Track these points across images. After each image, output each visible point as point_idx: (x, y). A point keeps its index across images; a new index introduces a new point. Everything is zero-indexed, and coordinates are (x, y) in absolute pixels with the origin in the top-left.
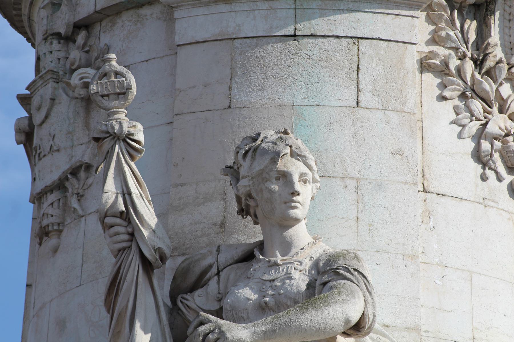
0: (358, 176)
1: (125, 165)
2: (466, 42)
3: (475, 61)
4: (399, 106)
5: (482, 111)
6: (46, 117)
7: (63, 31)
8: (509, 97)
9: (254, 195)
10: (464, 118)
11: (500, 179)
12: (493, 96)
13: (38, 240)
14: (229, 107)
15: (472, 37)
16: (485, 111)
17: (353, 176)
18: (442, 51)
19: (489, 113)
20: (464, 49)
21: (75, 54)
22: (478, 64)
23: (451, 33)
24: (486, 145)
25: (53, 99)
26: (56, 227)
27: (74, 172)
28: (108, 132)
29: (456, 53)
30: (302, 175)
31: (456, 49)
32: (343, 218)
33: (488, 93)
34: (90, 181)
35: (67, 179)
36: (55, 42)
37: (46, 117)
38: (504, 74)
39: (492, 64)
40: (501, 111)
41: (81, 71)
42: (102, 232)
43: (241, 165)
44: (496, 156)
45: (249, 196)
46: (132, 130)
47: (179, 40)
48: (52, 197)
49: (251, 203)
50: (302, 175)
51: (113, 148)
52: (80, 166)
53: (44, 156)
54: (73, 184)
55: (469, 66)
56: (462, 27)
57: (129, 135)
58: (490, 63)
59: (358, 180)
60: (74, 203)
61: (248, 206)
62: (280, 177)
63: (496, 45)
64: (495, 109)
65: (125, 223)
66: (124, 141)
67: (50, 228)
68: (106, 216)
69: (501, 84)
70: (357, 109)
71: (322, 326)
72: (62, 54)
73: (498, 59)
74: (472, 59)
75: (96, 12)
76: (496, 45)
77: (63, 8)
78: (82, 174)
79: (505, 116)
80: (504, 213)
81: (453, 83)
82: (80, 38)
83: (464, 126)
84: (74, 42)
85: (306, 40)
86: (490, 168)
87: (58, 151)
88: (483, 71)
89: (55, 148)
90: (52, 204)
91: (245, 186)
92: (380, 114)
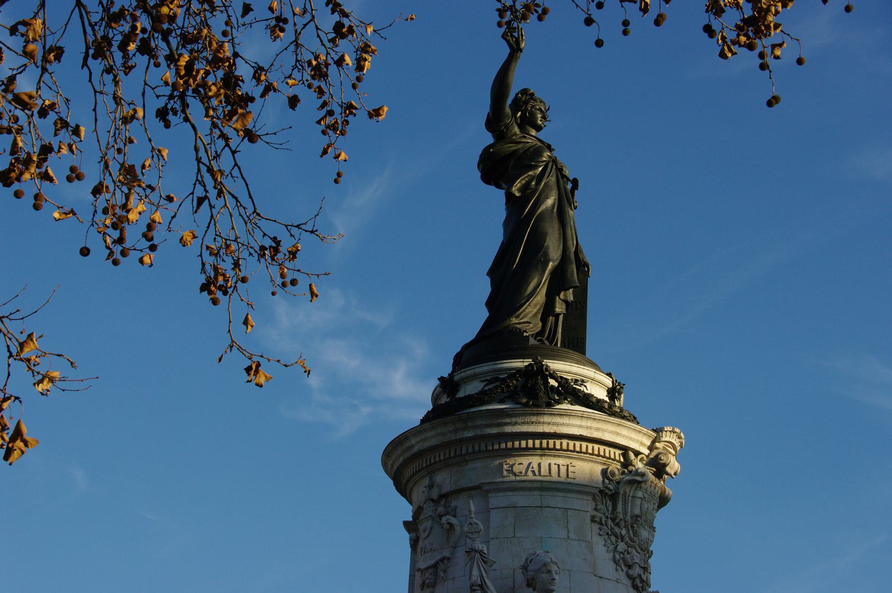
0: (569, 569)
1: (481, 565)
2: (608, 511)
3: (611, 519)
7: (435, 498)
8: (625, 535)
9: (535, 578)
10: (609, 544)
11: (622, 570)
12: (619, 535)
13: (421, 588)
14: (514, 537)
15: (610, 509)
16: (616, 541)
18: (599, 515)
19: (617, 541)
20: (607, 514)
21: (441, 509)
22: (613, 520)
23: (602, 507)
24: (617, 557)
25: (431, 528)
26: (432, 584)
27: (442, 560)
28: (472, 549)
29: (604, 515)
30: (556, 571)
31: (604, 514)
33: (617, 533)
35: (438, 563)
36: (431, 503)
37: (428, 536)
38: (623, 525)
39: (618, 521)
40: (622, 541)
41: (446, 517)
43: (529, 565)
44: (621, 561)
45: (533, 579)
46: (483, 549)
47: (490, 506)
48: (430, 571)
49: (533, 582)
50: (556, 571)
51: (475, 555)
52: (445, 558)
53: (427, 552)
54: (441, 566)
55: (610, 522)
56: (606, 504)
57: (482, 551)
58: (617, 521)
59: (569, 571)
60: (442, 574)
61: (532, 583)
63: (620, 513)
64: (620, 540)
65: (481, 589)
66: (479, 553)
67: (430, 584)
68: (473, 586)
69: (622, 529)
72: (434, 508)
73: (620, 519)
74: (611, 518)
75: (451, 491)
76: (620, 513)
77: (435, 488)
78: (446, 561)
79: (624, 543)
81: (603, 529)
82: (443, 502)
83: (608, 547)
84: (439, 503)
85: (546, 508)
86: (619, 566)
87: (434, 550)
88: (615, 523)
89: (433, 549)
90: (431, 574)
91: (531, 575)
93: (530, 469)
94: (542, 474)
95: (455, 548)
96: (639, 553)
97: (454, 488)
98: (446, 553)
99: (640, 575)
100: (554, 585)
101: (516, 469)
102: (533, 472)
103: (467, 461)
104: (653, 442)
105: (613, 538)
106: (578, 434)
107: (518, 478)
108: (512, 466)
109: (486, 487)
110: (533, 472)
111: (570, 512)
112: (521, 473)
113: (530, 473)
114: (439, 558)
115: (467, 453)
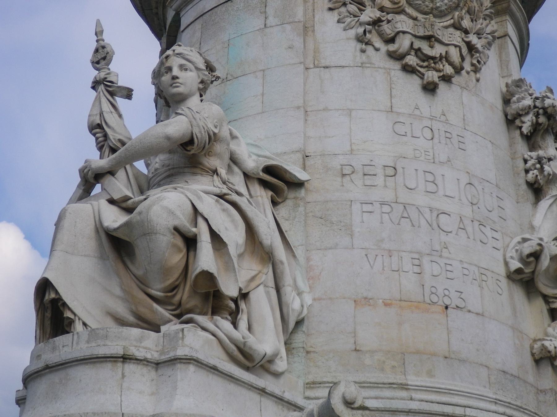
4: (291, 20)
5: (357, 10)
17: (261, 69)
32: (254, 96)
42: (217, 167)
59: (264, 71)
62: (168, 71)
70: (267, 30)
71: (148, 144)
80: (380, 70)
92: (279, 27)
96: (415, 19)
99: (418, 51)
100: (177, 87)
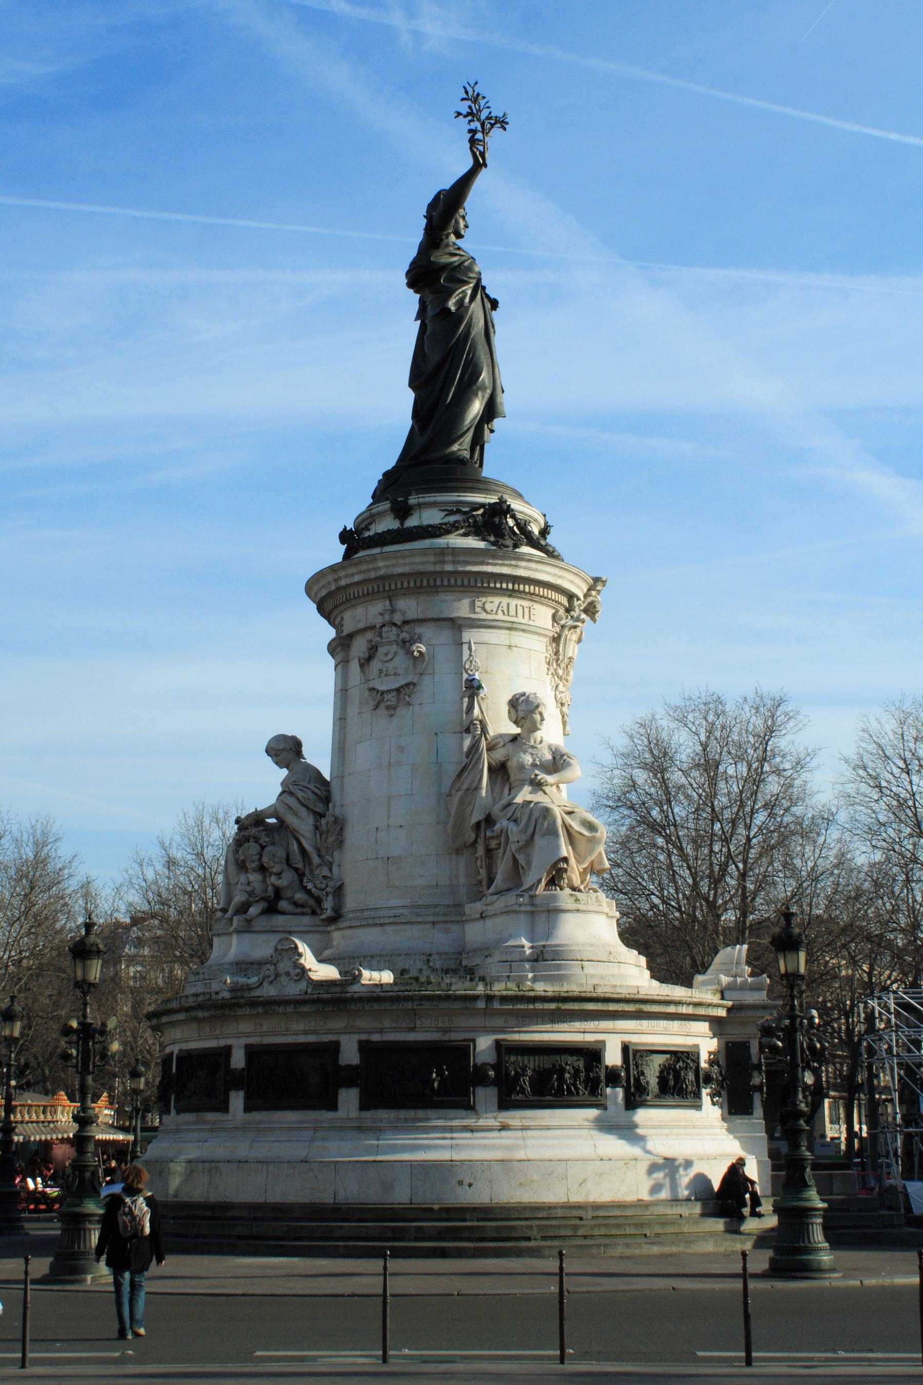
6: (392, 659)
27: (408, 685)
34: (415, 690)
37: (392, 659)
48: (394, 694)
78: (411, 687)
93: (500, 608)
94: (510, 614)
95: (421, 674)
97: (421, 616)
98: (409, 679)
101: (488, 607)
102: (503, 611)
103: (437, 592)
104: (589, 590)
105: (556, 678)
106: (527, 576)
107: (489, 617)
108: (484, 604)
109: (460, 622)
110: (503, 611)
111: (532, 652)
112: (492, 611)
113: (500, 612)
114: (404, 682)
115: (442, 585)
